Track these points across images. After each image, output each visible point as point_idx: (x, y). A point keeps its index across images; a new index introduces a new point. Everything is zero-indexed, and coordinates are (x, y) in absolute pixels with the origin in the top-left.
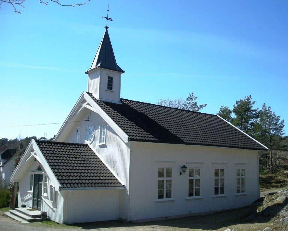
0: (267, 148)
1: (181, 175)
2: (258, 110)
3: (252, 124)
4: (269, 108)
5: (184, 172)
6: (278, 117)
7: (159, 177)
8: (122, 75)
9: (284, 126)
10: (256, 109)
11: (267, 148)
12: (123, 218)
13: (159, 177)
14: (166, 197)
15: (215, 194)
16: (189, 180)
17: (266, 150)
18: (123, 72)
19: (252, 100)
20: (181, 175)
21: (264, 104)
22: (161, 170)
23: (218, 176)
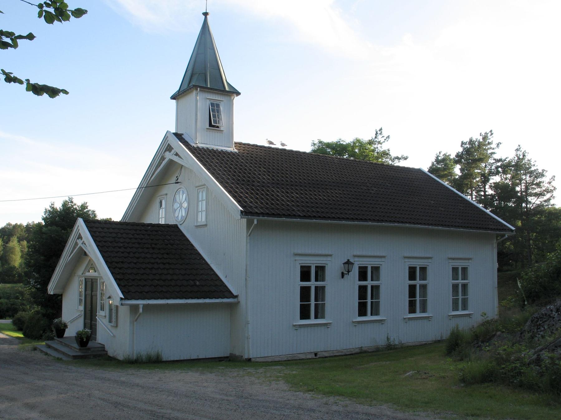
0: (513, 228)
1: (343, 277)
2: (508, 160)
3: (496, 186)
4: (320, 142)
5: (349, 272)
6: (543, 170)
7: (301, 281)
8: (236, 100)
9: (555, 189)
10: (503, 158)
11: (513, 228)
12: (237, 353)
13: (301, 281)
14: (316, 317)
15: (360, 315)
16: (301, 287)
17: (512, 231)
18: (238, 94)
19: (494, 140)
20: (343, 277)
21: (519, 146)
22: (305, 269)
23: (309, 280)
